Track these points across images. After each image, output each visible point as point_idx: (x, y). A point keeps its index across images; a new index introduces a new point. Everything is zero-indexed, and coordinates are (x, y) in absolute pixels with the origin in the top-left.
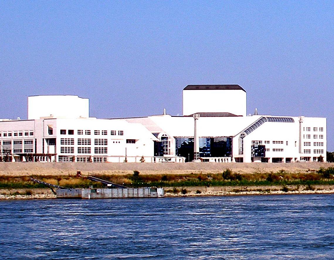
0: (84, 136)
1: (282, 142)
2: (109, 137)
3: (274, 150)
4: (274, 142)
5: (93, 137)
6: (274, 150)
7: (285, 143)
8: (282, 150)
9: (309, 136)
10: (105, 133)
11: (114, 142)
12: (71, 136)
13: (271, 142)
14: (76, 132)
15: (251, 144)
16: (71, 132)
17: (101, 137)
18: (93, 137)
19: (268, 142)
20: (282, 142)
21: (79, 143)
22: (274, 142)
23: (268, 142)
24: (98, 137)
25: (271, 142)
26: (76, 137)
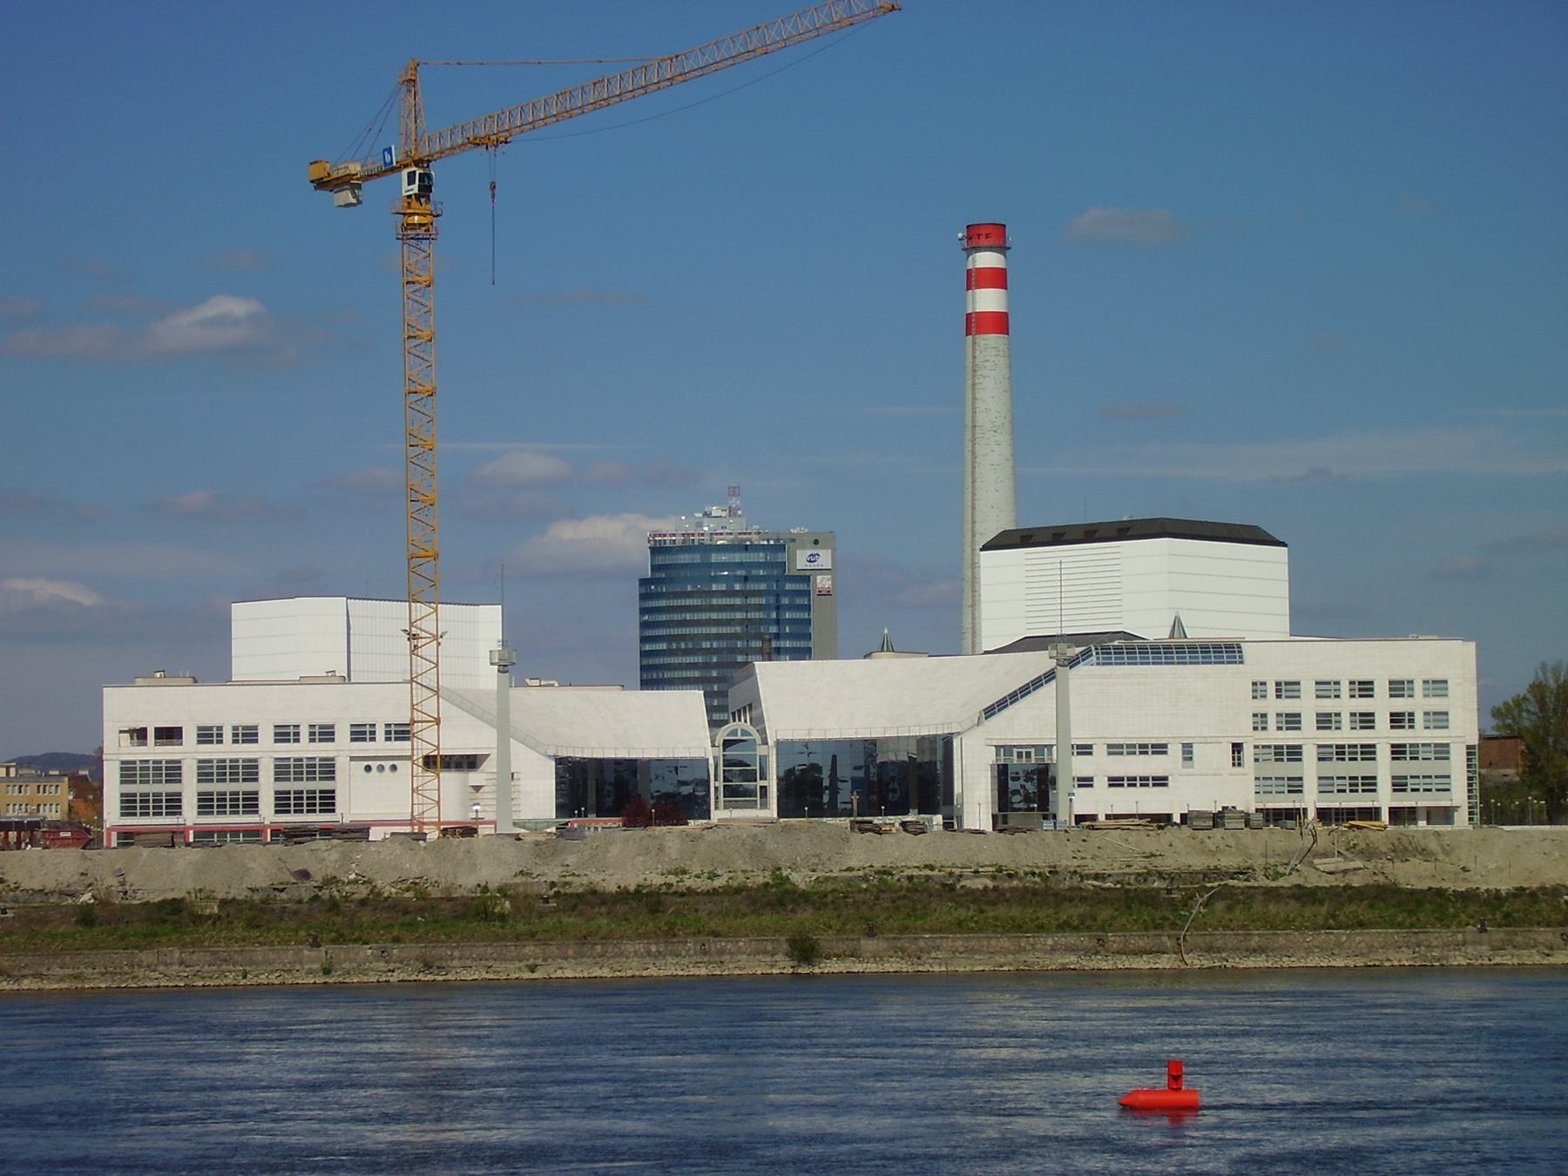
0: (227, 750)
1: (1160, 749)
2: (341, 748)
3: (1115, 782)
4: (1114, 749)
5: (266, 751)
6: (1115, 782)
7: (1175, 750)
8: (1161, 781)
9: (1366, 720)
10: (325, 733)
11: (368, 768)
12: (166, 752)
13: (1100, 750)
14: (190, 736)
15: (990, 757)
16: (169, 735)
17: (305, 749)
18: (266, 751)
20: (1160, 749)
21: (204, 775)
22: (1114, 749)
24: (289, 750)
26: (189, 752)
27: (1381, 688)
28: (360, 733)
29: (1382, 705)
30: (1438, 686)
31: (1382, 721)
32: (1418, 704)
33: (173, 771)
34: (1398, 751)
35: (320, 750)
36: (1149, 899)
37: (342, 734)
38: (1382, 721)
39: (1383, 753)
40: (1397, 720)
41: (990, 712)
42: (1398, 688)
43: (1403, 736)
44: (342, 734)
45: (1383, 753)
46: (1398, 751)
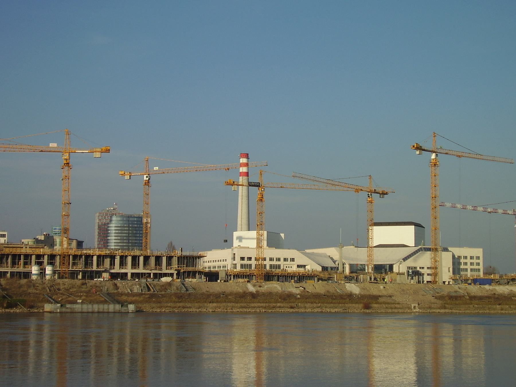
10: (279, 259)
13: (426, 268)
19: (423, 268)
23: (423, 268)
24: (272, 263)
25: (426, 268)
27: (469, 258)
28: (285, 260)
29: (469, 261)
30: (478, 258)
31: (469, 264)
32: (475, 261)
33: (251, 265)
34: (471, 270)
35: (278, 263)
36: (456, 298)
37: (282, 260)
38: (469, 264)
39: (469, 270)
40: (472, 264)
41: (405, 259)
42: (472, 258)
43: (472, 267)
44: (282, 260)
45: (469, 270)
46: (471, 270)
